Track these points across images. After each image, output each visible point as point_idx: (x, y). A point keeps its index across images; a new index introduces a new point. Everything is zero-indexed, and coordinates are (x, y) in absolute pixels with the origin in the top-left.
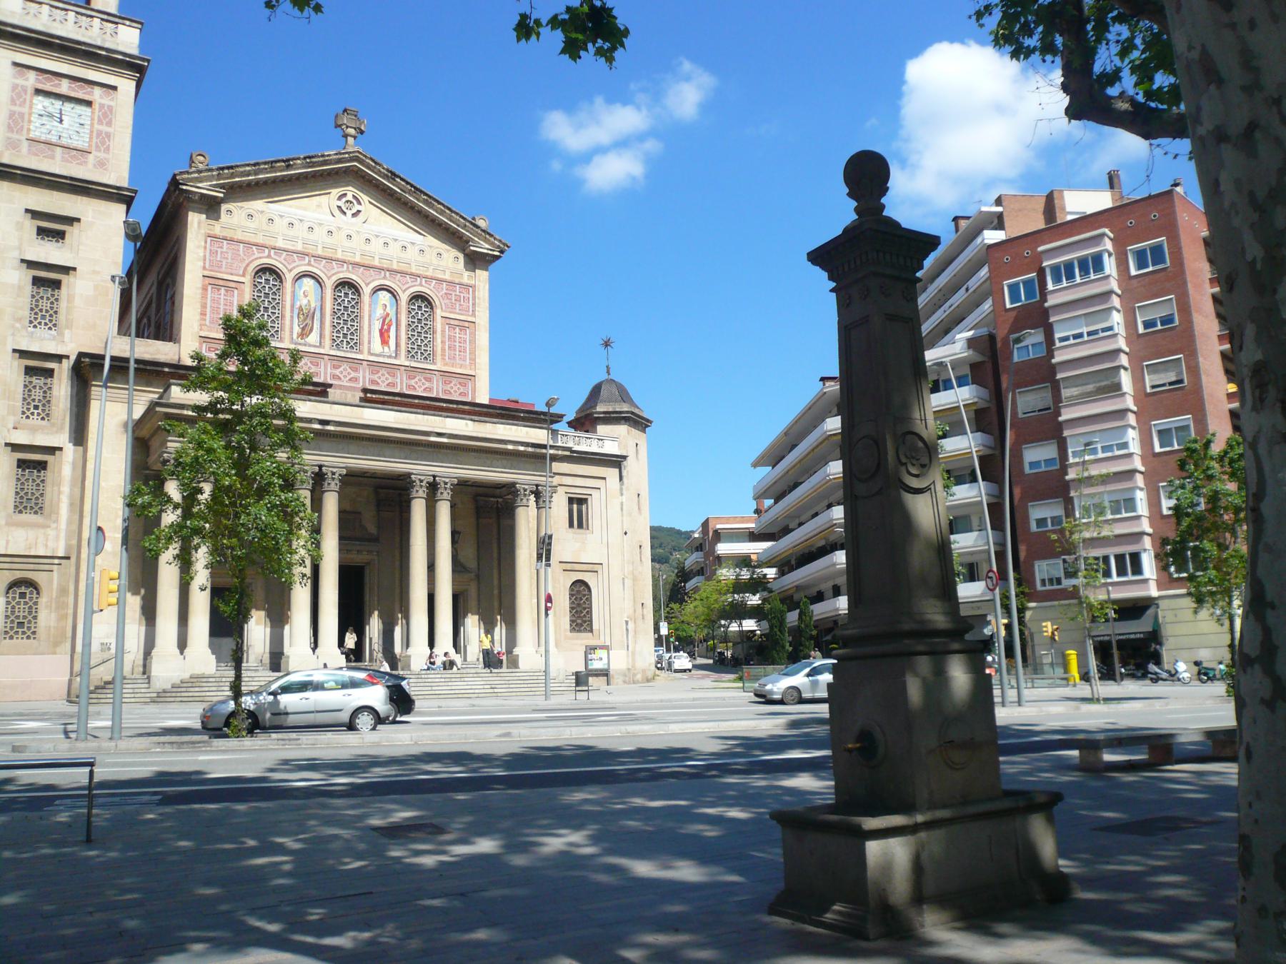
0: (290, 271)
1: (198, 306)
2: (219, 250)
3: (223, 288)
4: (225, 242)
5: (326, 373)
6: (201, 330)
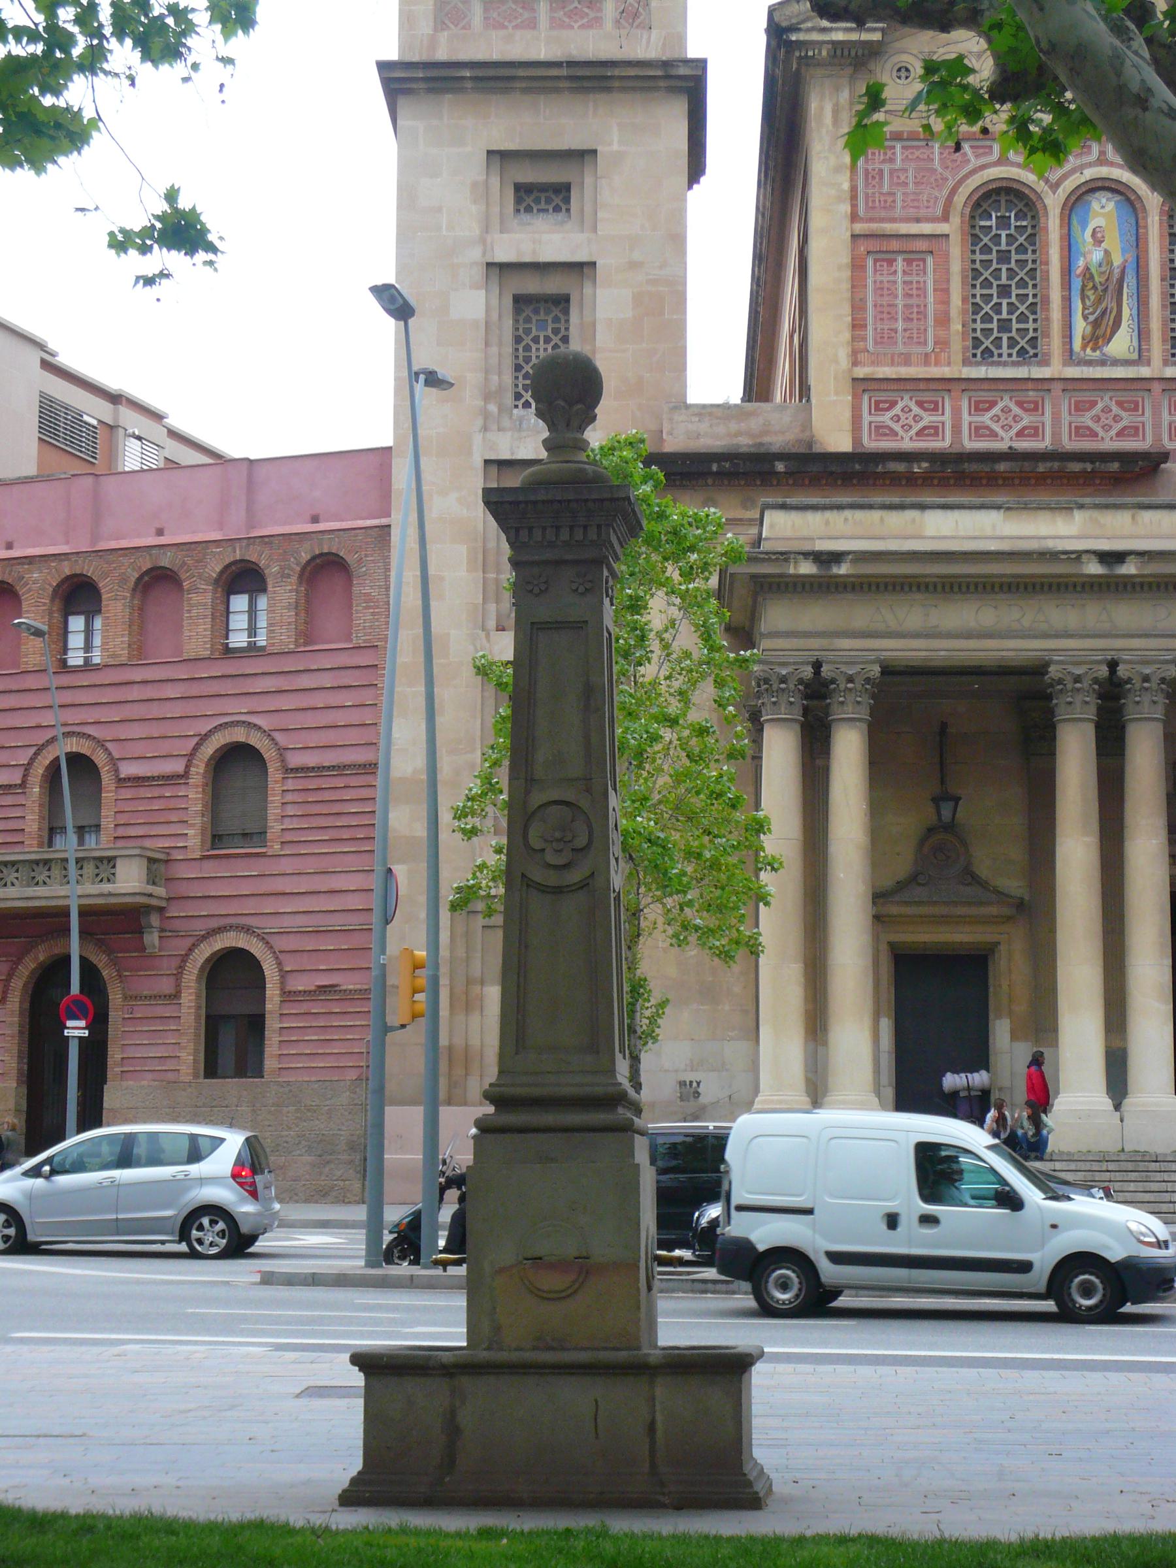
0: (1055, 187)
1: (847, 309)
2: (886, 168)
3: (900, 259)
4: (898, 146)
5: (1157, 426)
6: (855, 363)
